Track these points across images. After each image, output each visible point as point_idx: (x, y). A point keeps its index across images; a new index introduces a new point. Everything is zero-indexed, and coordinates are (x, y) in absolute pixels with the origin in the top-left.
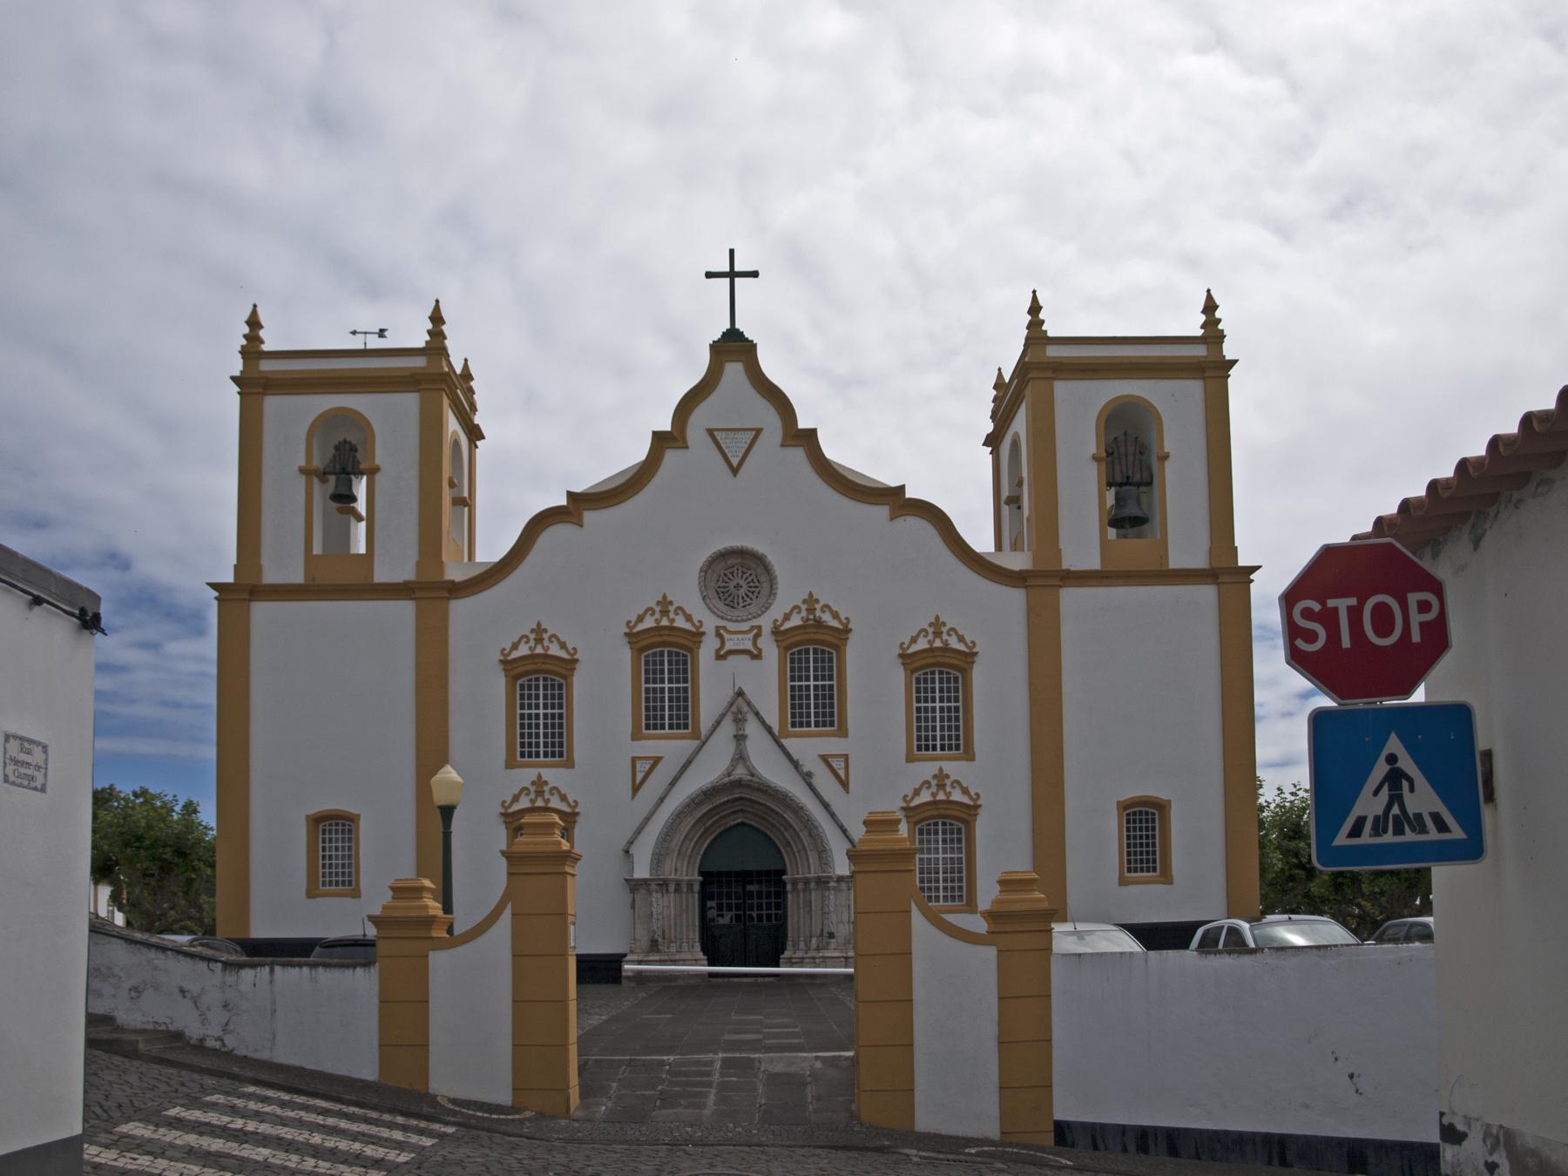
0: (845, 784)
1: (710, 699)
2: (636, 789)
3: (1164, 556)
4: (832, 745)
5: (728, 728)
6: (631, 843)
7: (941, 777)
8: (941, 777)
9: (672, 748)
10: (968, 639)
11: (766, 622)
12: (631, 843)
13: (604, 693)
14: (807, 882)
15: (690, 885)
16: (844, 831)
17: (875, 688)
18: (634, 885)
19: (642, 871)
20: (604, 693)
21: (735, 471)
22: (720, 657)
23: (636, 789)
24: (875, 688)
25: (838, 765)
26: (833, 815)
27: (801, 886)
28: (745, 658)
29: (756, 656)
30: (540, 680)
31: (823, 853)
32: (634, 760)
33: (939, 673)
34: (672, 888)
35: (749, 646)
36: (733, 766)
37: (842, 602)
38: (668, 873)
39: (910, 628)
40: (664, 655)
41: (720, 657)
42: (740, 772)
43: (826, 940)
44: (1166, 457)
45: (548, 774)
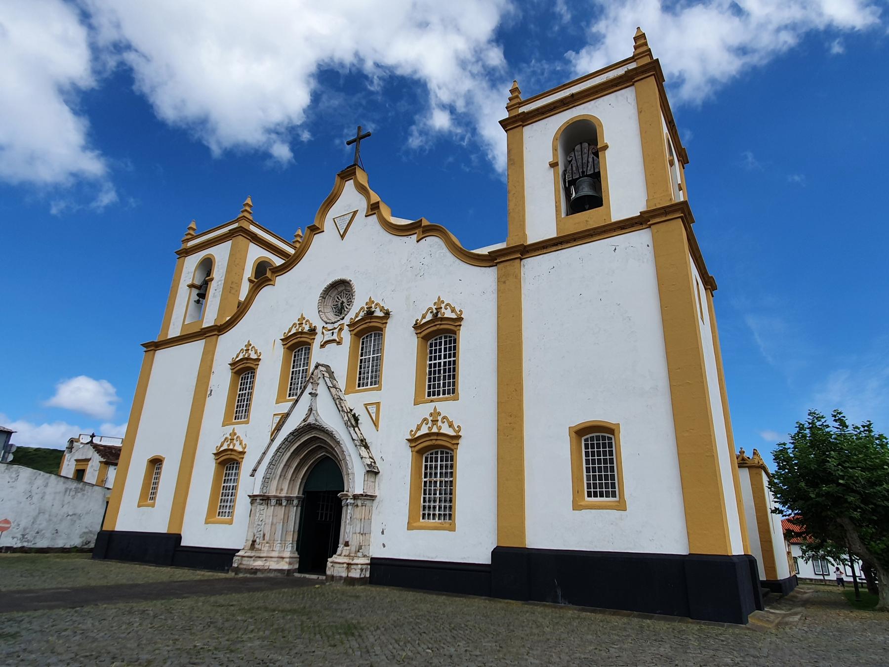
0: (376, 424)
4: (370, 396)
6: (255, 470)
7: (435, 414)
8: (435, 414)
10: (457, 310)
11: (347, 321)
12: (255, 470)
15: (289, 500)
17: (401, 350)
18: (253, 498)
21: (342, 236)
24: (401, 350)
25: (372, 410)
28: (335, 344)
29: (339, 343)
34: (273, 502)
35: (335, 337)
36: (308, 416)
38: (272, 492)
41: (322, 346)
42: (311, 420)
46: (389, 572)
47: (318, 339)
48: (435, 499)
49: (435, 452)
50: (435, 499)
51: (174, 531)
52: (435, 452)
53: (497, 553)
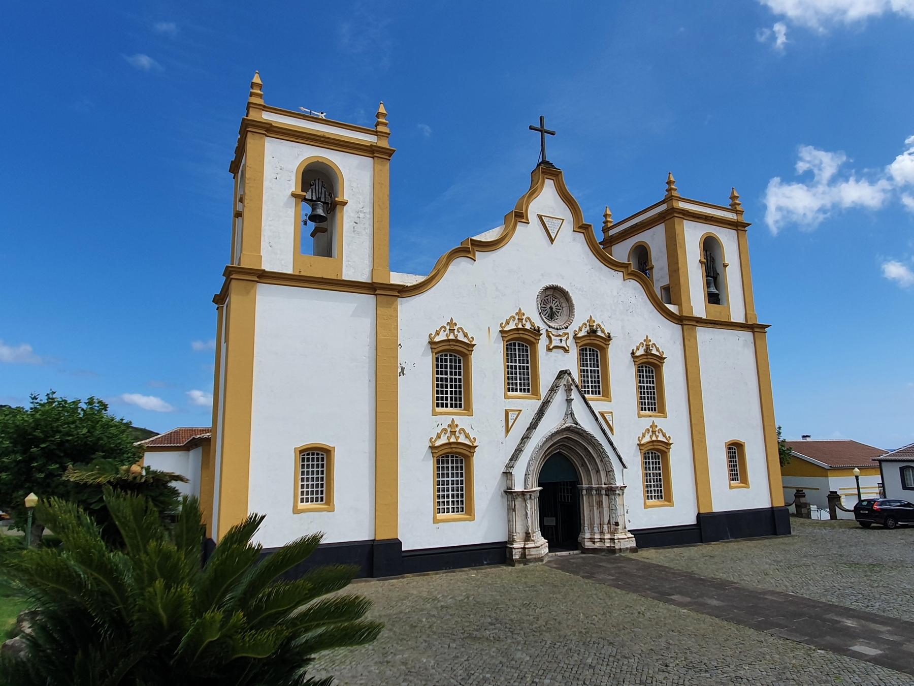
0: (611, 429)
1: (546, 373)
2: (507, 431)
3: (729, 316)
5: (560, 396)
9: (528, 406)
11: (571, 331)
13: (488, 365)
14: (599, 490)
16: (620, 459)
19: (518, 487)
20: (488, 365)
22: (549, 350)
23: (507, 431)
26: (614, 449)
27: (594, 492)
28: (561, 351)
29: (566, 351)
30: (452, 357)
31: (609, 472)
32: (507, 413)
33: (649, 366)
35: (563, 344)
37: (608, 326)
39: (635, 342)
40: (520, 345)
41: (549, 350)
43: (613, 527)
44: (725, 266)
45: (458, 420)
46: (647, 538)
47: (543, 342)
48: (658, 487)
49: (656, 454)
50: (658, 487)
51: (384, 535)
52: (656, 454)
53: (699, 516)
